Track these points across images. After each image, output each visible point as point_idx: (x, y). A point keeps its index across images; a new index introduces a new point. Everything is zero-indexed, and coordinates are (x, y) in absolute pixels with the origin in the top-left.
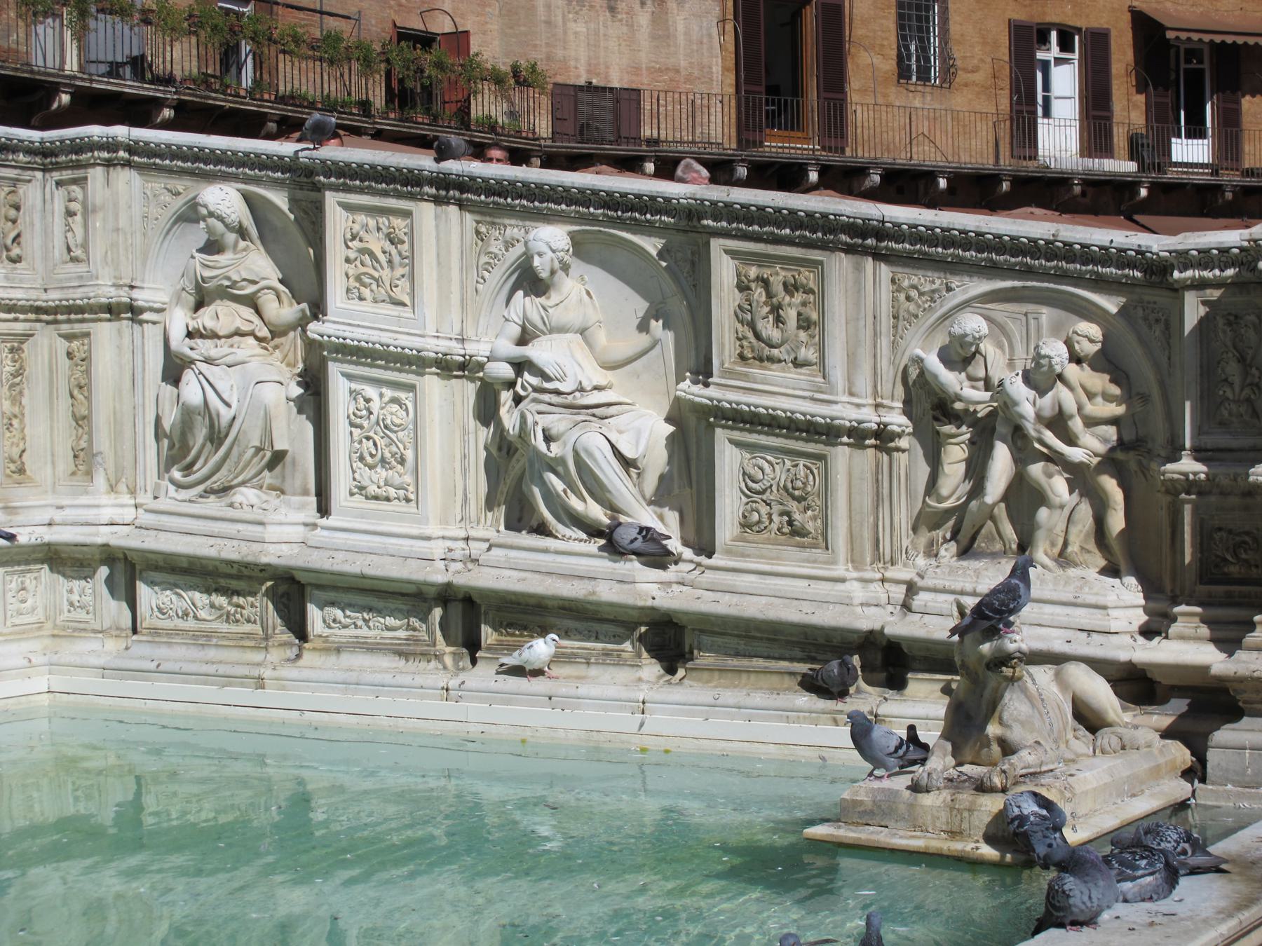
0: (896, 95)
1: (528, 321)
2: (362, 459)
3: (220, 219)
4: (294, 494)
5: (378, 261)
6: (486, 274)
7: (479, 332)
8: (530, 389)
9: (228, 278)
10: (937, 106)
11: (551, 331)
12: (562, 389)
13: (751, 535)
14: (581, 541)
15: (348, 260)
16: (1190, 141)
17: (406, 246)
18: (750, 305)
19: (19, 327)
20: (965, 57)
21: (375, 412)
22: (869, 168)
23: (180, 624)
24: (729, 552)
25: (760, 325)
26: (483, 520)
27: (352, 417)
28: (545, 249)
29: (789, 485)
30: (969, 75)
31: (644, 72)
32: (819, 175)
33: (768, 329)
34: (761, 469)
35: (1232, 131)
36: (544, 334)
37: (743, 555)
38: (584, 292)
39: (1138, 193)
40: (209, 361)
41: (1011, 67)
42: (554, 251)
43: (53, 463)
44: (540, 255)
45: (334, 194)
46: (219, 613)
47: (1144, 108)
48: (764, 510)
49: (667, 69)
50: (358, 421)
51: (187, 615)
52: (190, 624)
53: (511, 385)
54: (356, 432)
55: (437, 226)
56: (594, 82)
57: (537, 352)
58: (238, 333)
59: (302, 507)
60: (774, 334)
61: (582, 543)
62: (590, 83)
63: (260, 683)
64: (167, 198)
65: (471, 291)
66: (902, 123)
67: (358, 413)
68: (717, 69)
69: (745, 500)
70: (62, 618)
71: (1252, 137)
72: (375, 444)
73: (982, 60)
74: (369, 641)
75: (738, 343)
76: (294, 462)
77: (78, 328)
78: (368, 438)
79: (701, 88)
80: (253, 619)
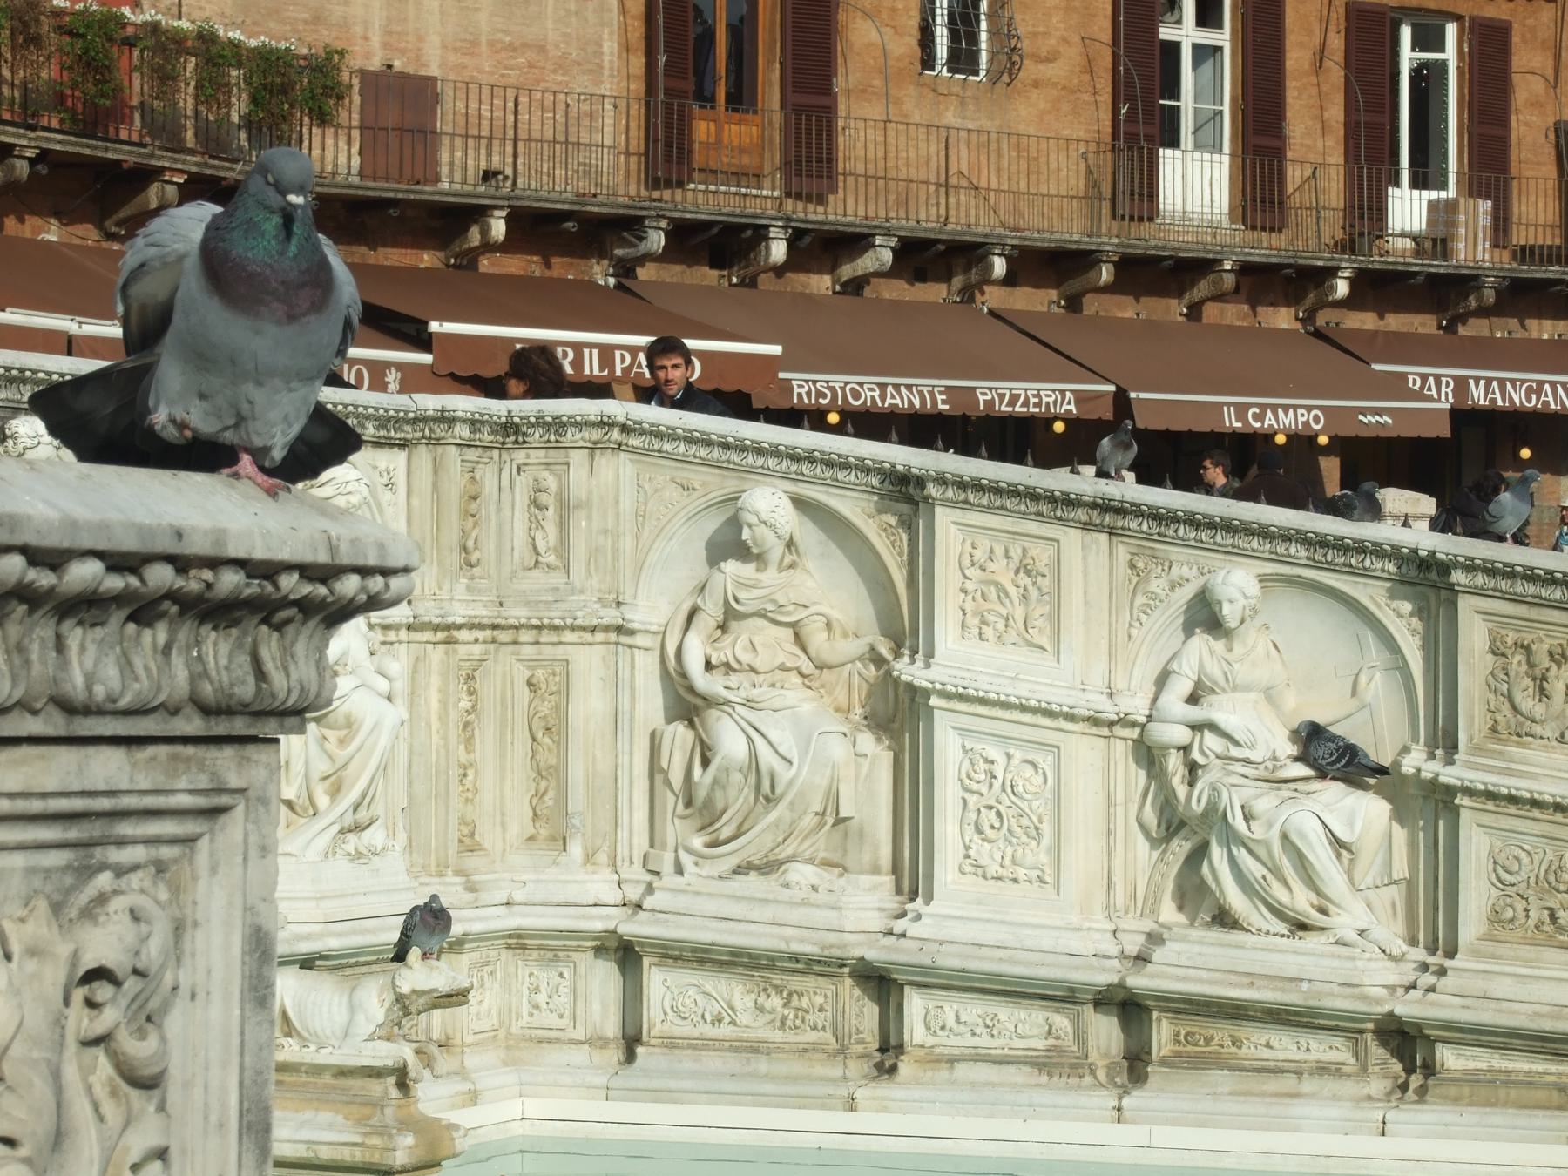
0: (914, 106)
1: (1206, 676)
2: (979, 831)
3: (771, 527)
4: (861, 872)
5: (1007, 595)
6: (1143, 617)
7: (1134, 683)
8: (1212, 756)
9: (774, 601)
10: (987, 124)
11: (1235, 688)
12: (1253, 759)
13: (1500, 933)
14: (1283, 936)
15: (964, 591)
16: (1416, 193)
17: (1045, 583)
18: (1506, 674)
19: (477, 650)
20: (1035, 35)
21: (999, 773)
22: (874, 235)
23: (710, 1031)
24: (1476, 954)
25: (1518, 697)
26: (1132, 909)
27: (967, 782)
28: (1236, 595)
29: (1552, 878)
30: (1041, 67)
31: (484, 48)
32: (789, 246)
33: (1527, 702)
34: (1517, 859)
35: (1488, 179)
36: (1224, 690)
37: (1493, 957)
38: (1271, 645)
39: (1332, 289)
40: (748, 703)
41: (1115, 56)
42: (1246, 597)
43: (503, 824)
44: (1231, 602)
45: (948, 510)
46: (768, 1017)
47: (1342, 132)
48: (1520, 905)
49: (525, 45)
50: (975, 786)
51: (720, 1021)
52: (725, 1031)
53: (1185, 749)
54: (972, 799)
55: (1084, 558)
56: (398, 64)
57: (1219, 710)
58: (783, 668)
59: (874, 888)
60: (1539, 710)
61: (1285, 939)
62: (390, 67)
63: (851, 1105)
64: (674, 493)
65: (1121, 635)
66: (923, 152)
67: (973, 775)
68: (610, 46)
69: (1495, 892)
70: (521, 1023)
71: (1524, 188)
72: (999, 814)
73: (1065, 40)
74: (993, 1052)
75: (1490, 714)
76: (861, 833)
77: (548, 651)
78: (990, 808)
79: (583, 84)
80: (820, 1026)
